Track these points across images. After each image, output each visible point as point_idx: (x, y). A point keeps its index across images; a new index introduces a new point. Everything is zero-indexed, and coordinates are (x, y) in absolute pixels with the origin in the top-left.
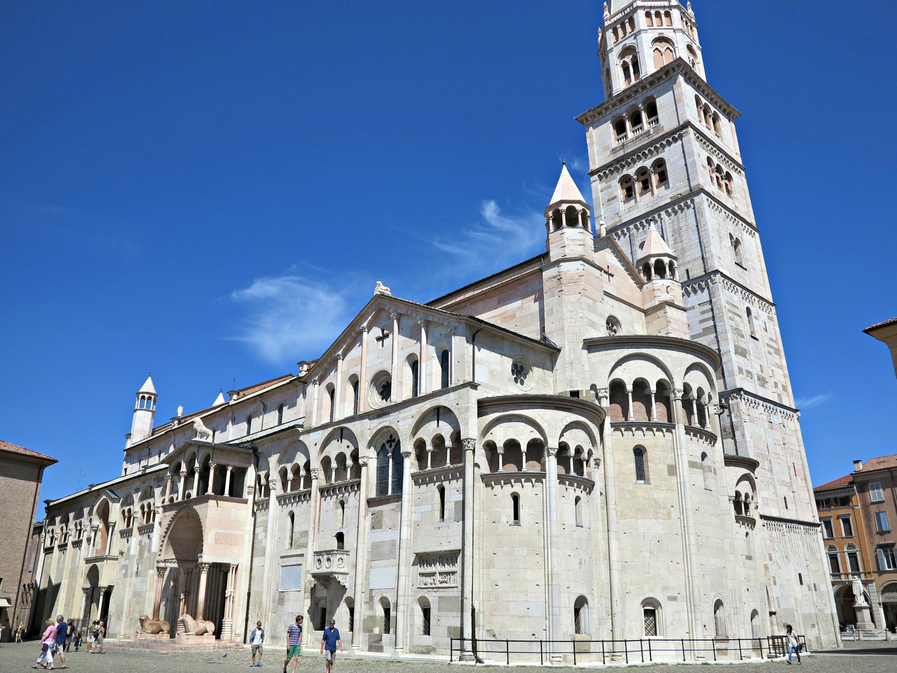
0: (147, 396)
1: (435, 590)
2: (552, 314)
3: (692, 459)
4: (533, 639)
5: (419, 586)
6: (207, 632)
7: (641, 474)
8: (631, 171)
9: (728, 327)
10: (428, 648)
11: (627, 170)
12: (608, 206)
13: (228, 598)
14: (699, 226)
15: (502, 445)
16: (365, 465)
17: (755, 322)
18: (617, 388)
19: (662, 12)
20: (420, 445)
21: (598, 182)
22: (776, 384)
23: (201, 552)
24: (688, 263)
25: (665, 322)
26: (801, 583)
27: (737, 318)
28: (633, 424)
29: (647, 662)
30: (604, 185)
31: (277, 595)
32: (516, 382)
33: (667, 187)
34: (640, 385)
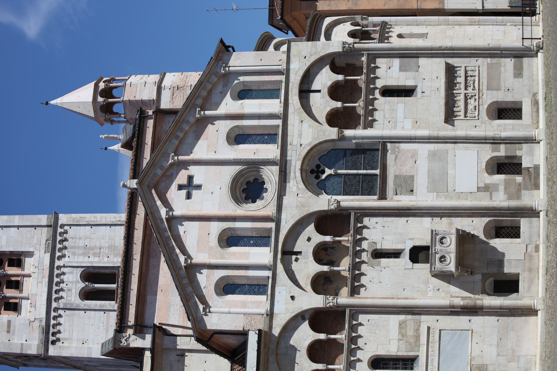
1: (481, 95)
5: (477, 118)
10: (533, 103)
12: (14, 334)
14: (93, 223)
15: (353, 39)
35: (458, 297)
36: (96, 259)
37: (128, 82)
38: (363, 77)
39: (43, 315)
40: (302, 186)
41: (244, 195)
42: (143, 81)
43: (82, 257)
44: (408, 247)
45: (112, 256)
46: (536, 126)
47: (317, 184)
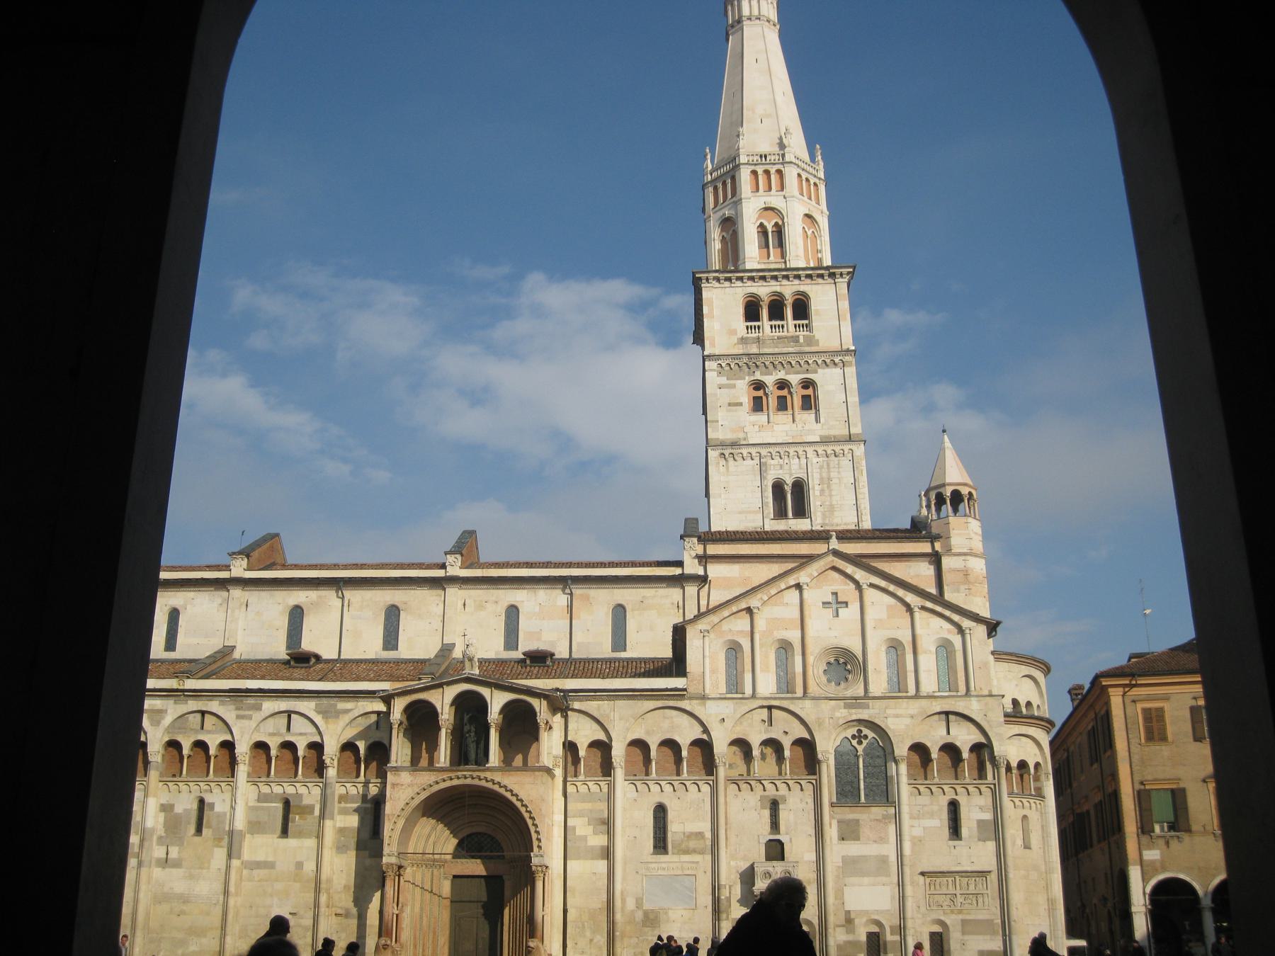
11: (761, 374)
12: (728, 411)
19: (812, 180)
21: (715, 374)
30: (723, 380)
31: (639, 915)
33: (817, 420)
35: (730, 893)
36: (817, 493)
37: (970, 520)
38: (967, 781)
39: (751, 443)
40: (841, 722)
41: (832, 660)
42: (973, 535)
43: (819, 477)
45: (822, 510)
47: (846, 737)
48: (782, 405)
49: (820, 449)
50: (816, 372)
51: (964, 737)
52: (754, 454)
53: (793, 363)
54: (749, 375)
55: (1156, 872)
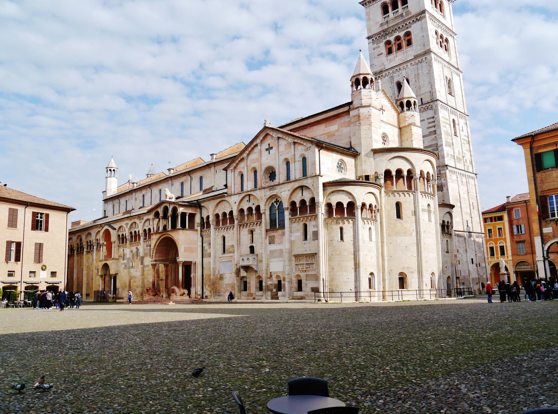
0: (112, 169)
2: (355, 135)
3: (423, 208)
4: (351, 291)
6: (185, 294)
7: (399, 216)
8: (392, 38)
9: (442, 132)
13: (193, 278)
16: (264, 213)
17: (457, 126)
18: (388, 173)
20: (293, 204)
21: (372, 44)
22: (466, 160)
23: (178, 256)
24: (422, 94)
25: (411, 135)
26: (473, 263)
27: (448, 126)
28: (395, 191)
29: (401, 300)
30: (375, 45)
31: (219, 276)
32: (339, 172)
34: (399, 172)
36: (414, 82)
40: (268, 197)
44: (254, 245)
46: (293, 298)
47: (273, 203)
48: (400, 47)
49: (413, 62)
50: (411, 27)
51: (307, 197)
52: (387, 74)
53: (401, 27)
54: (384, 39)
55: (550, 238)
